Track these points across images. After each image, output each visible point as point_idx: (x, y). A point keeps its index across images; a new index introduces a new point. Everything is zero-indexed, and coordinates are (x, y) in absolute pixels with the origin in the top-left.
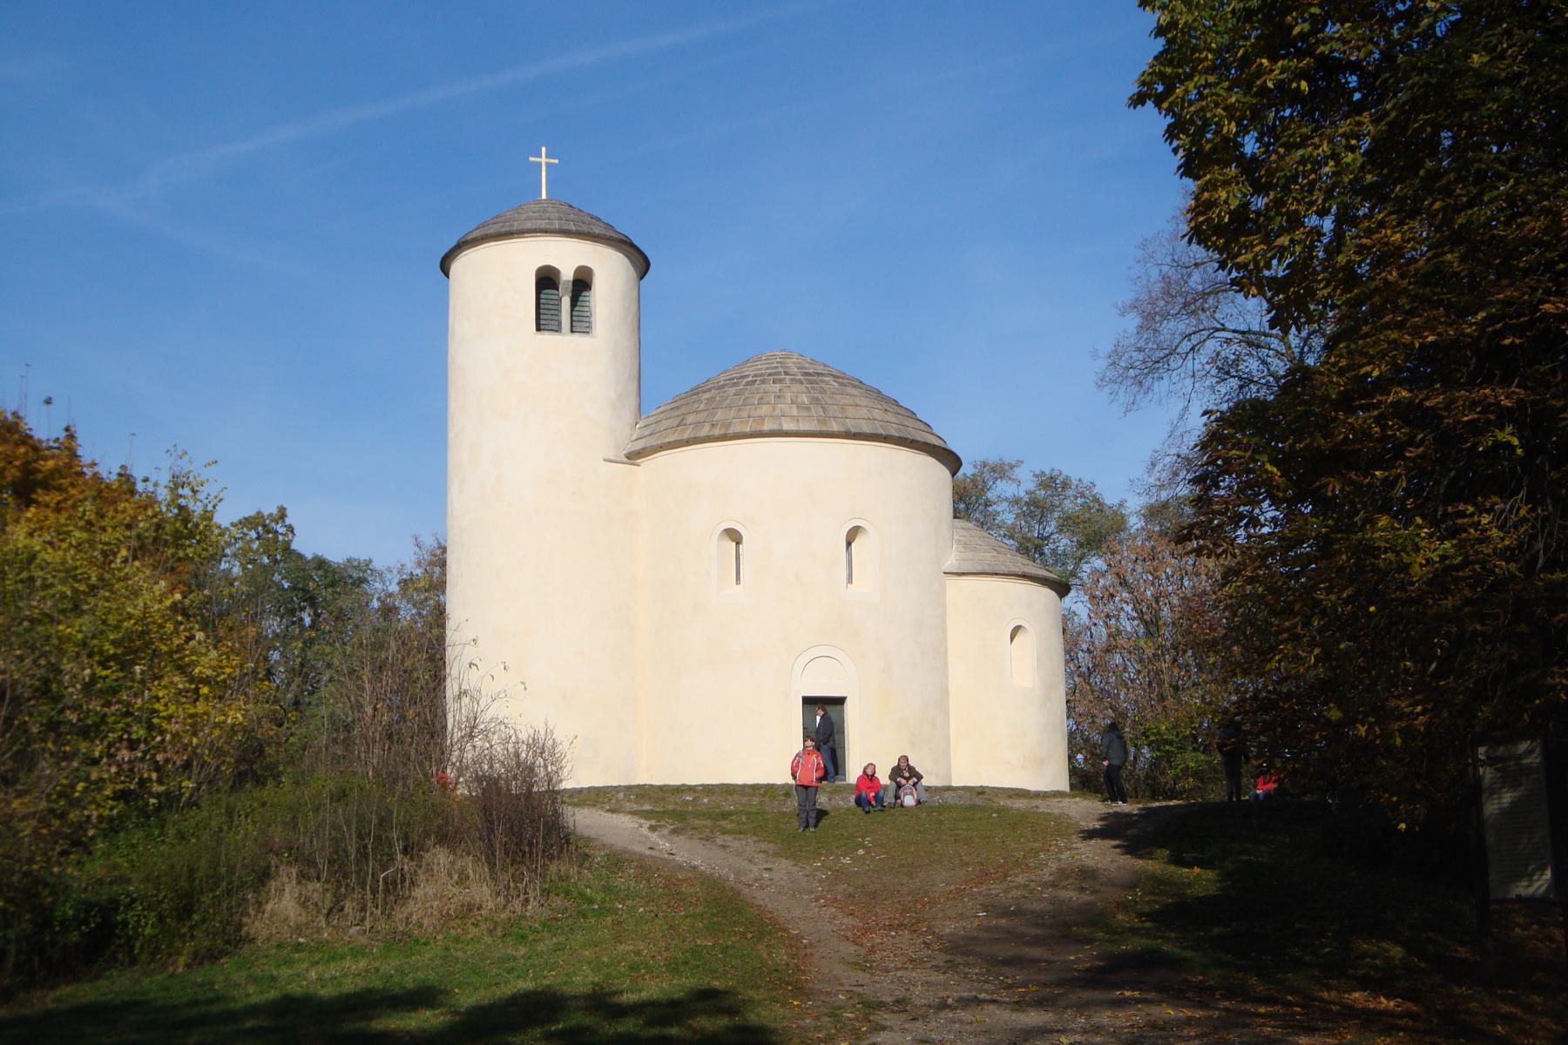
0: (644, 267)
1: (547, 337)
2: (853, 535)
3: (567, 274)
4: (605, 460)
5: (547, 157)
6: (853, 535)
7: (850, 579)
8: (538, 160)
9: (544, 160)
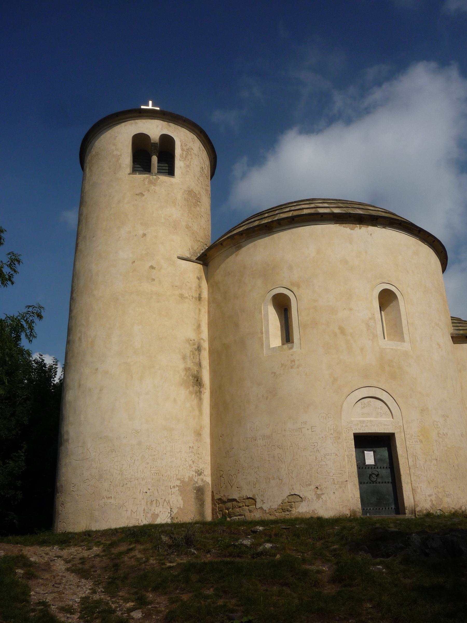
1: (140, 177)
4: (179, 258)
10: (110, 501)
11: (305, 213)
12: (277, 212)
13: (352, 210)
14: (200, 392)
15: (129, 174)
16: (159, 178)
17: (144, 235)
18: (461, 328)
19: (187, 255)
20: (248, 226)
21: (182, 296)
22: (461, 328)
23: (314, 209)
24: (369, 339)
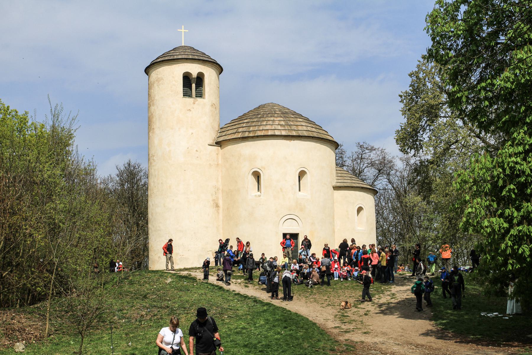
1: (188, 100)
2: (302, 174)
3: (195, 75)
4: (209, 145)
6: (302, 174)
7: (300, 190)
8: (183, 32)
9: (183, 30)
10: (183, 256)
12: (256, 128)
13: (291, 132)
14: (218, 210)
16: (197, 100)
17: (192, 133)
18: (340, 181)
19: (211, 141)
21: (210, 164)
22: (340, 181)
23: (273, 131)
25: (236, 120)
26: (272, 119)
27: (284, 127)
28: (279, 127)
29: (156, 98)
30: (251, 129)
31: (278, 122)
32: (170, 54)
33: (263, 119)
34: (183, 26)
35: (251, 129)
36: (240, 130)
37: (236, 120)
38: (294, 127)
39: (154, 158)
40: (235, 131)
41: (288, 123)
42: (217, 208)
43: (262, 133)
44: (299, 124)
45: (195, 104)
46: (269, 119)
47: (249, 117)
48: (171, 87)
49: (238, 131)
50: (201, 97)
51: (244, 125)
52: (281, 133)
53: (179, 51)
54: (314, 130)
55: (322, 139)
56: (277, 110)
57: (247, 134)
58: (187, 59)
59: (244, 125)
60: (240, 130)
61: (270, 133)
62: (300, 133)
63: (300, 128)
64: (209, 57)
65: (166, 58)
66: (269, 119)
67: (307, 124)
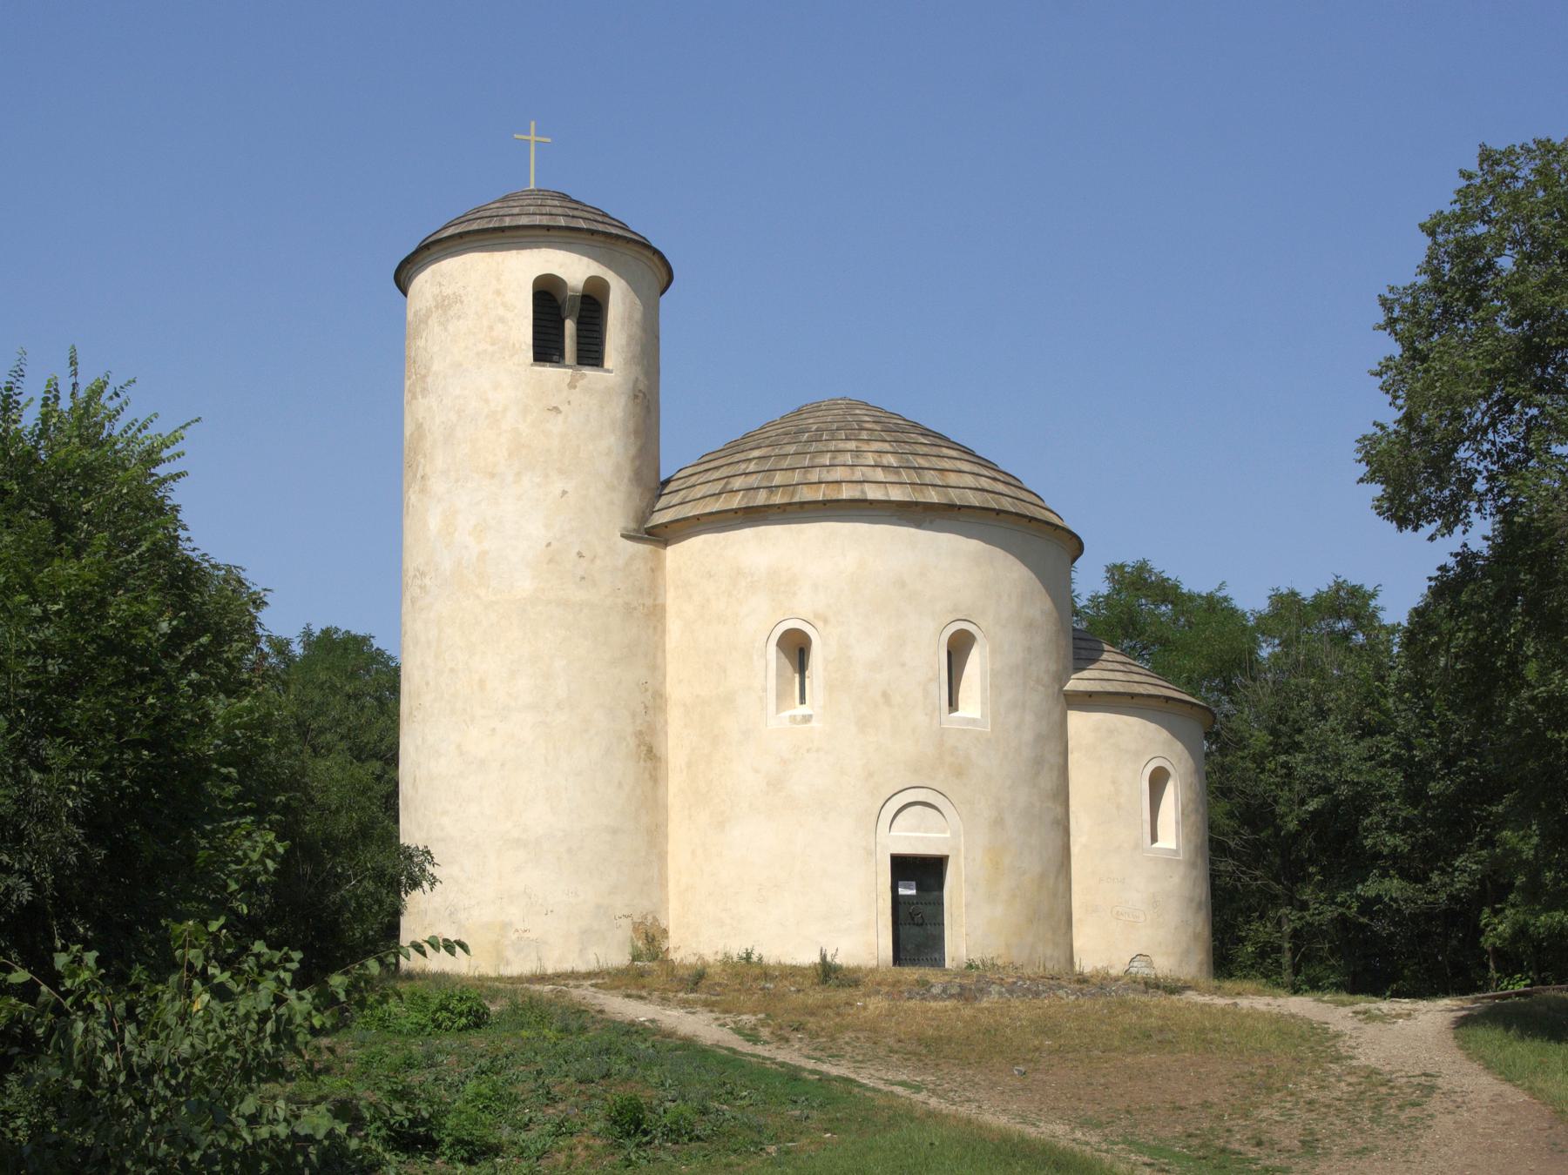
0: (666, 279)
1: (549, 372)
5: (536, 135)
8: (538, 139)
9: (532, 138)
10: (526, 935)
11: (844, 497)
12: (797, 477)
13: (922, 491)
14: (655, 769)
15: (532, 365)
17: (564, 493)
20: (746, 500)
23: (859, 487)
24: (926, 714)
25: (722, 454)
26: (852, 445)
27: (898, 474)
28: (880, 475)
29: (435, 367)
30: (778, 478)
31: (876, 455)
32: (488, 213)
33: (821, 446)
34: (533, 124)
35: (778, 478)
36: (737, 483)
37: (722, 454)
38: (930, 477)
39: (427, 581)
40: (718, 487)
41: (908, 460)
42: (649, 764)
43: (819, 494)
44: (947, 464)
45: (575, 387)
46: (842, 445)
47: (767, 442)
48: (491, 328)
49: (729, 487)
50: (597, 366)
51: (752, 467)
52: (887, 494)
53: (521, 203)
54: (1000, 487)
55: (1032, 519)
56: (867, 419)
57: (761, 498)
58: (548, 228)
59: (752, 467)
60: (737, 483)
61: (846, 493)
62: (955, 497)
63: (953, 479)
64: (625, 228)
65: (475, 226)
66: (842, 445)
67: (976, 469)
